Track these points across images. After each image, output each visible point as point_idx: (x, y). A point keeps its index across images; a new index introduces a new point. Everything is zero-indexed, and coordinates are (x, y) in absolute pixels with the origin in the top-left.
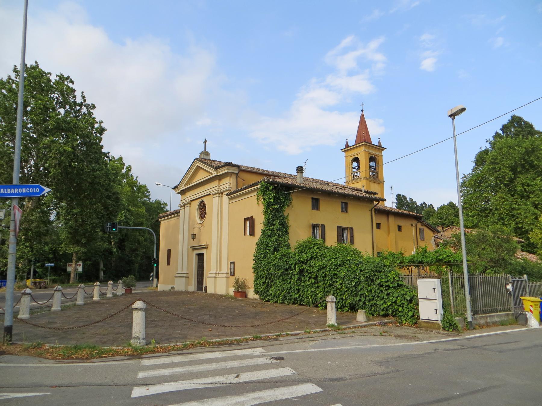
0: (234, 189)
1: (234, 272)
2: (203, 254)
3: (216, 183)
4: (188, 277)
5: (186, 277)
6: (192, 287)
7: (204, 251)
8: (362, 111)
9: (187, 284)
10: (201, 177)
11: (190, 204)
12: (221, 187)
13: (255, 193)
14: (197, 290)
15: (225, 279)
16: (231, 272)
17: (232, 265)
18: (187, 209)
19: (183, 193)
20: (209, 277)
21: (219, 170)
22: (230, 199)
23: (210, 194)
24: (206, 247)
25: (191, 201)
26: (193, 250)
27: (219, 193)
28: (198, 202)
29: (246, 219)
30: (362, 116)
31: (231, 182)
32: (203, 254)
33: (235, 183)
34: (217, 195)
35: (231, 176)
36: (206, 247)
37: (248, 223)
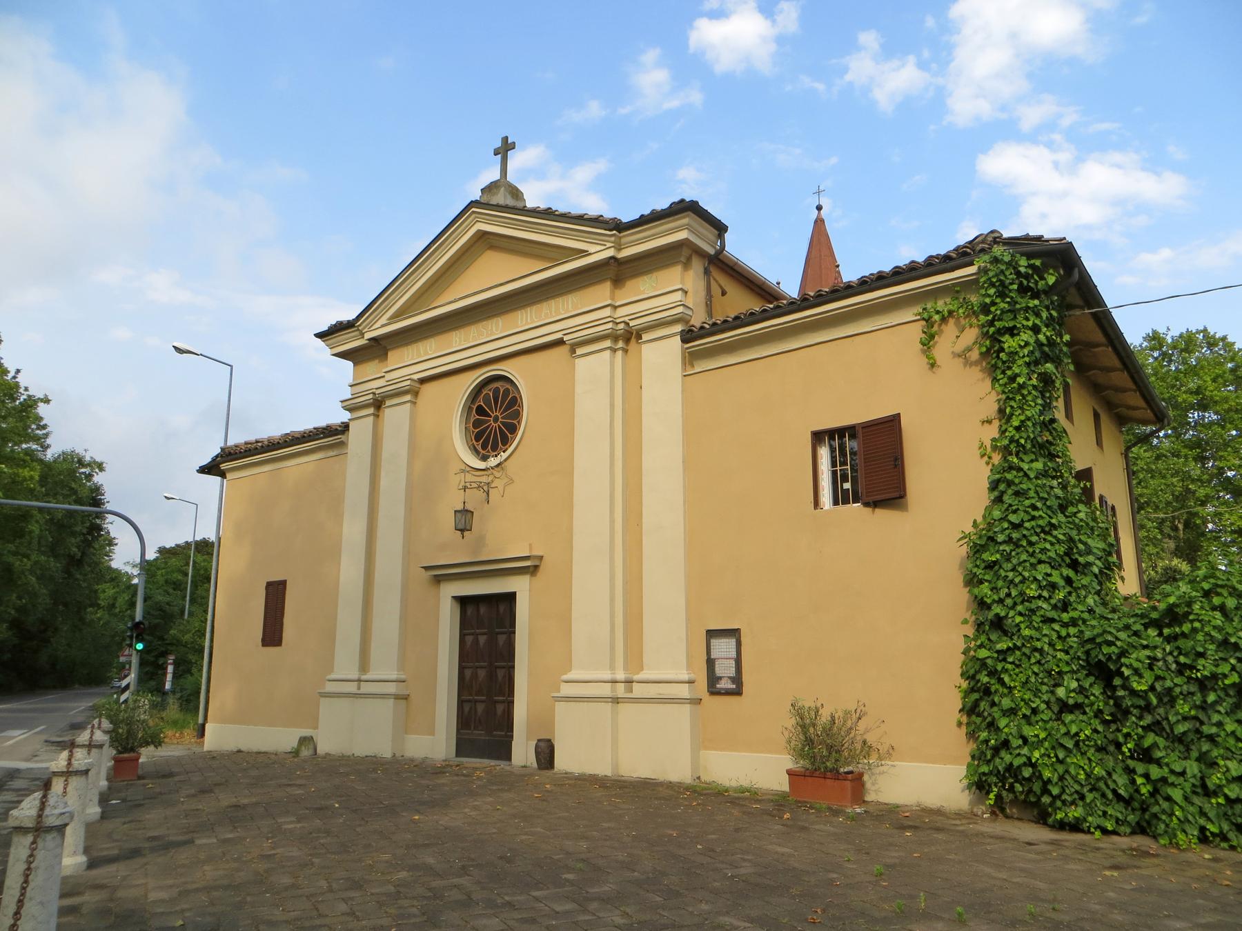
0: (699, 319)
1: (738, 679)
2: (511, 598)
3: (601, 293)
4: (406, 698)
5: (397, 697)
6: (435, 740)
7: (519, 585)
8: (819, 208)
9: (404, 726)
10: (493, 275)
11: (416, 394)
12: (621, 312)
13: (909, 314)
14: (459, 753)
15: (687, 708)
16: (713, 679)
17: (724, 649)
18: (396, 415)
19: (378, 349)
20: (568, 699)
21: (628, 237)
22: (691, 358)
23: (560, 342)
24: (531, 567)
25: (423, 381)
26: (438, 580)
27: (615, 338)
28: (470, 381)
29: (818, 437)
30: (819, 223)
31: (688, 286)
32: (511, 598)
33: (703, 293)
34: (608, 343)
35: (687, 265)
36: (531, 567)
37: (824, 453)
